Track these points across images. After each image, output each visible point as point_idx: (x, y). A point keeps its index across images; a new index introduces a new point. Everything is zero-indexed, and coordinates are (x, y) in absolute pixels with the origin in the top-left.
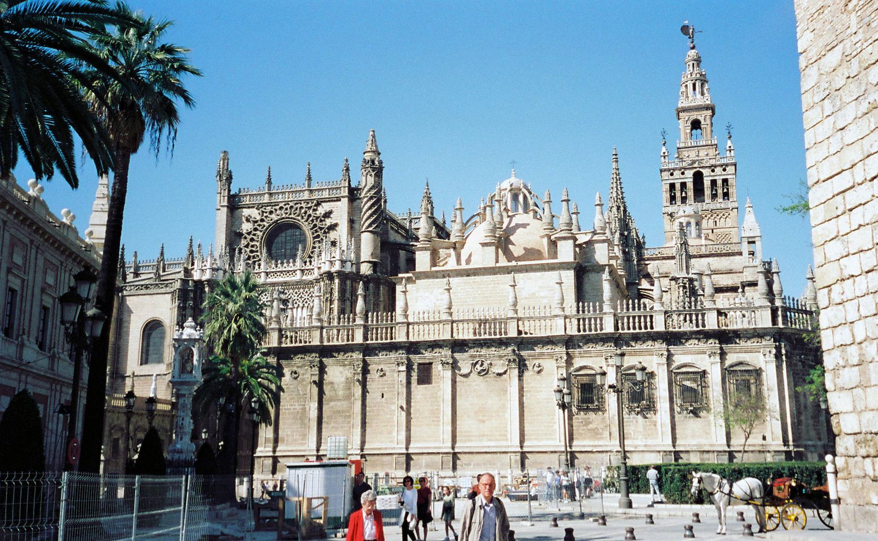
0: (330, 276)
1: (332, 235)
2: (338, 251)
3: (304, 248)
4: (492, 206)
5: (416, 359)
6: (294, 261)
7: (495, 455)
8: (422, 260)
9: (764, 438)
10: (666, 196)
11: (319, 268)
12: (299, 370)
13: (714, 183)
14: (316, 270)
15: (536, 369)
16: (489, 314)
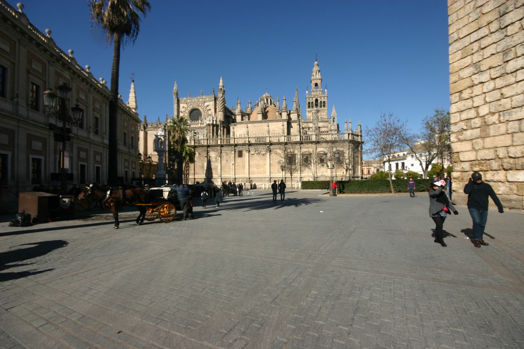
0: (209, 125)
1: (210, 112)
2: (211, 117)
3: (201, 117)
4: (261, 101)
5: (238, 149)
6: (198, 121)
7: (262, 179)
8: (239, 118)
9: (343, 173)
10: (307, 106)
11: (206, 123)
12: (201, 153)
13: (321, 102)
14: (205, 123)
15: (275, 153)
16: (260, 136)
